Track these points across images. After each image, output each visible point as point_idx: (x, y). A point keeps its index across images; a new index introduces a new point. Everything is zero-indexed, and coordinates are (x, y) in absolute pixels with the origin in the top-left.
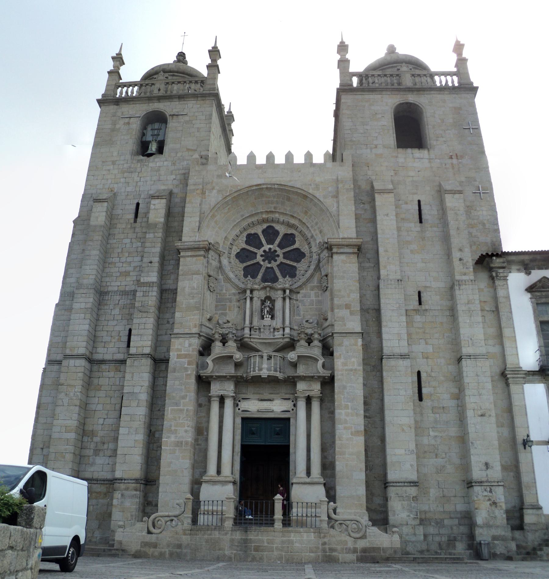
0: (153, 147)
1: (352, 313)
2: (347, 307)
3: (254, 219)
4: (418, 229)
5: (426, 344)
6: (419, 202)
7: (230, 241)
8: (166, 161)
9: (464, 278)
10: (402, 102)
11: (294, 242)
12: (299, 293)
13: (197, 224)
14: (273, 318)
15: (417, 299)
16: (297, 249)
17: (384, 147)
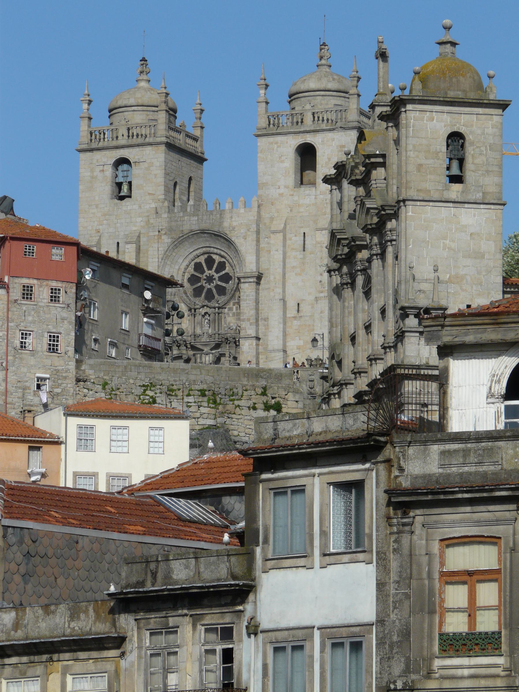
0: (125, 188)
1: (251, 324)
2: (249, 320)
3: (198, 252)
4: (301, 256)
5: (300, 339)
6: (304, 233)
7: (183, 270)
8: (134, 204)
9: (322, 295)
10: (301, 143)
11: (224, 268)
12: (225, 308)
13: (157, 264)
14: (209, 327)
15: (297, 309)
16: (227, 274)
17: (286, 187)
